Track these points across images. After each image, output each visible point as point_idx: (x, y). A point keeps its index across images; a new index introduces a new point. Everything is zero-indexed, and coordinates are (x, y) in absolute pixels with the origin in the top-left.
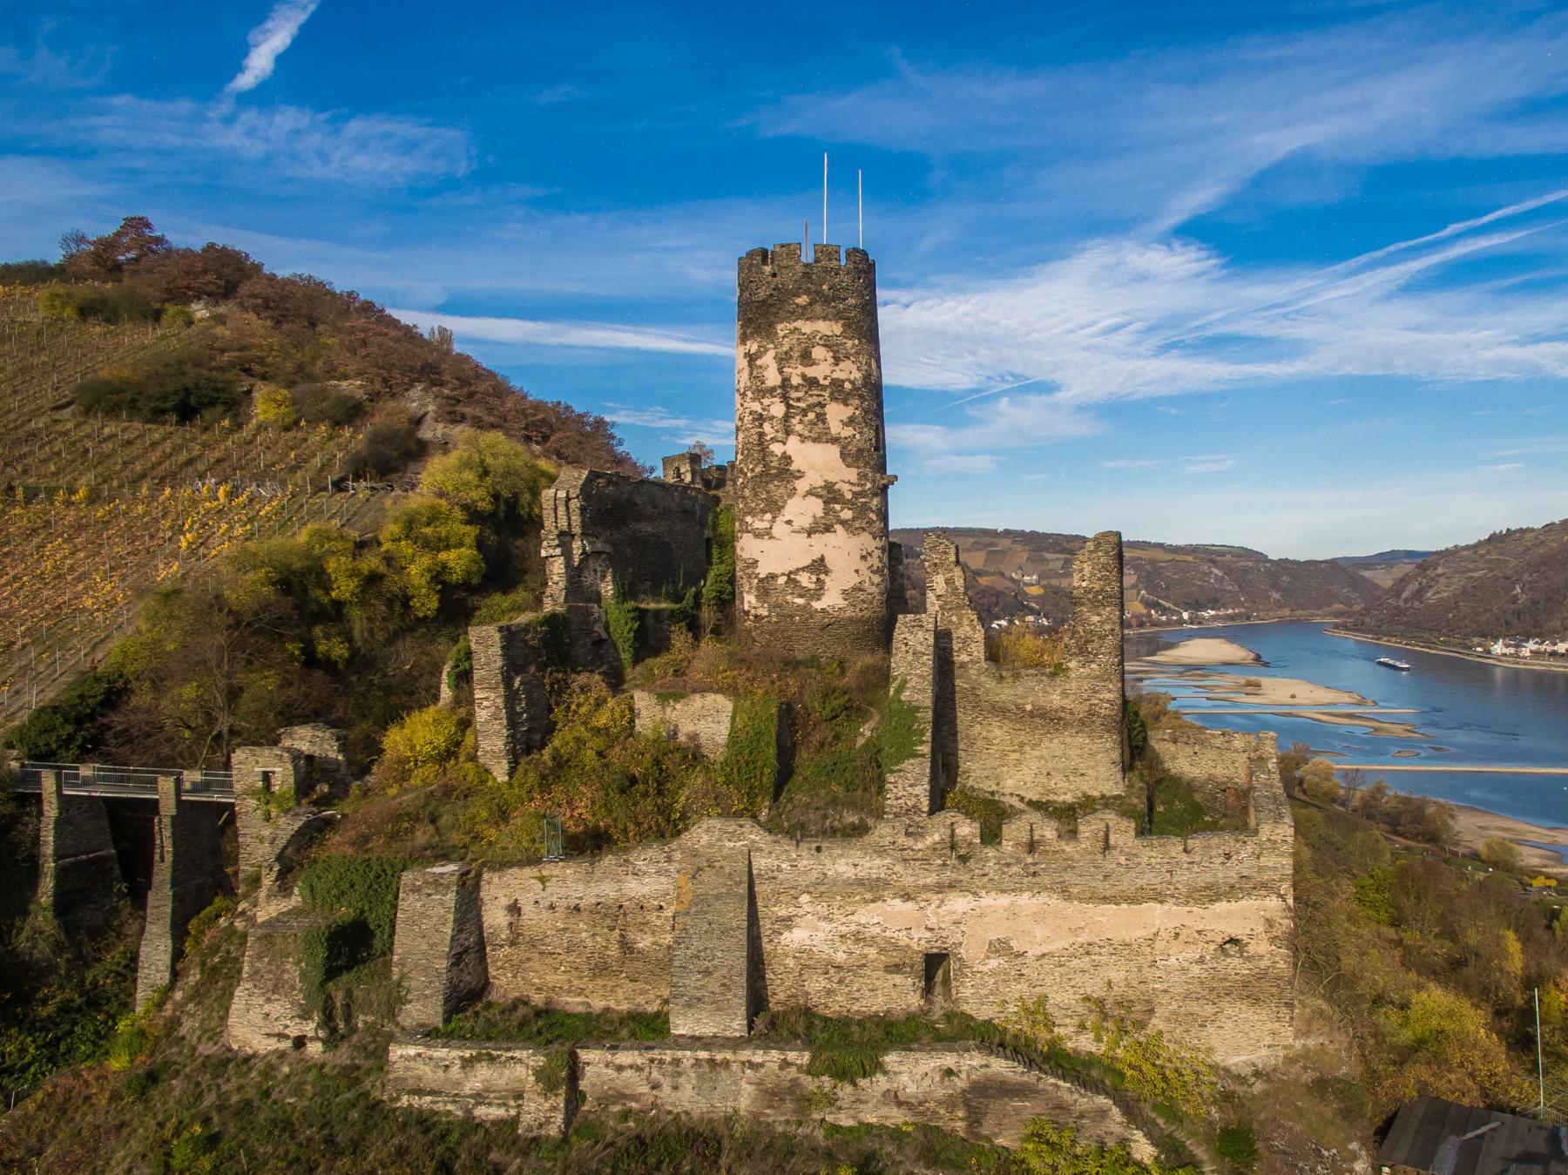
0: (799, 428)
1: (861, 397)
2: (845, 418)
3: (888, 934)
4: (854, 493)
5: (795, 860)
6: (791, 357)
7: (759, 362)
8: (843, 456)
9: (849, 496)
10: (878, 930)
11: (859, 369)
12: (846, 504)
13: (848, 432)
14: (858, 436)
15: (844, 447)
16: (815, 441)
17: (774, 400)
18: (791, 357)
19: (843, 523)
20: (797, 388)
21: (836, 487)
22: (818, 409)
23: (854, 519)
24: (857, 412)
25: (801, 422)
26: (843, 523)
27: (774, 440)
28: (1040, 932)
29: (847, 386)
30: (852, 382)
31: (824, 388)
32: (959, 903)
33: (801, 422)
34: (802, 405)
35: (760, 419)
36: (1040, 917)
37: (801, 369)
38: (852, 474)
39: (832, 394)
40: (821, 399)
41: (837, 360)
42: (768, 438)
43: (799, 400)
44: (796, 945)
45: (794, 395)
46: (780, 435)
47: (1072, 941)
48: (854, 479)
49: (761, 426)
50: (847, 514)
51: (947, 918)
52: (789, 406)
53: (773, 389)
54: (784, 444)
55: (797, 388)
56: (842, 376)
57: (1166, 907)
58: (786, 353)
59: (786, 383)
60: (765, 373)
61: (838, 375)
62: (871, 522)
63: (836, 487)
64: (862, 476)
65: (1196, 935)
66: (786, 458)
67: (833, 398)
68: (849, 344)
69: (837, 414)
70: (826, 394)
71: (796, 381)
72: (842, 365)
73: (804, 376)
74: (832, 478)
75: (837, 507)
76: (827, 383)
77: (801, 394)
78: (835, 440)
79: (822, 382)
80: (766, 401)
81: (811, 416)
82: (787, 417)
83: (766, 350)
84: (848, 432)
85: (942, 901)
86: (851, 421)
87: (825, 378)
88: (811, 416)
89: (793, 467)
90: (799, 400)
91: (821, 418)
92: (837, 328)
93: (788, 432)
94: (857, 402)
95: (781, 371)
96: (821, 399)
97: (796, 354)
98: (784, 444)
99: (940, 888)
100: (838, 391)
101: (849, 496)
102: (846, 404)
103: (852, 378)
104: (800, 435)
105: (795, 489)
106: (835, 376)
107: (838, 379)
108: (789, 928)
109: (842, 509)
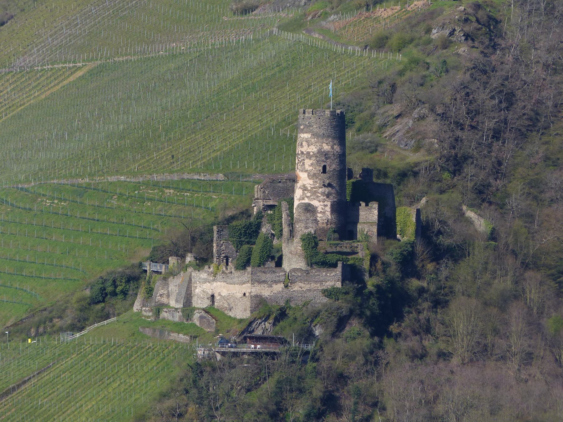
1: (317, 157)
2: (310, 164)
8: (308, 176)
9: (309, 188)
11: (316, 148)
12: (308, 191)
14: (314, 169)
15: (309, 173)
19: (307, 197)
22: (303, 161)
23: (311, 196)
26: (307, 197)
29: (311, 153)
38: (311, 182)
41: (309, 146)
50: (309, 194)
62: (318, 197)
67: (307, 158)
68: (313, 140)
72: (310, 147)
75: (306, 192)
78: (306, 171)
81: (302, 163)
84: (311, 168)
86: (312, 164)
88: (302, 163)
91: (304, 163)
94: (314, 158)
101: (309, 188)
102: (310, 159)
103: (313, 151)
106: (308, 151)
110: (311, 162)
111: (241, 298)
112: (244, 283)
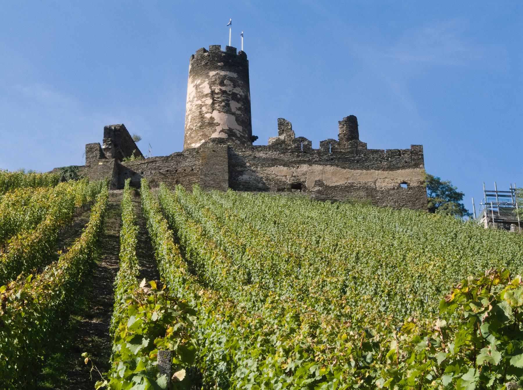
0: (218, 108)
3: (278, 177)
4: (241, 135)
5: (245, 152)
6: (216, 83)
7: (201, 86)
8: (237, 120)
10: (274, 176)
13: (239, 112)
14: (243, 116)
16: (224, 112)
17: (207, 98)
18: (216, 83)
20: (217, 94)
21: (234, 131)
24: (242, 107)
25: (219, 106)
27: (206, 113)
28: (334, 179)
30: (241, 96)
31: (229, 95)
32: (305, 168)
33: (219, 106)
34: (220, 100)
35: (201, 106)
36: (334, 174)
37: (219, 87)
38: (240, 128)
39: (232, 97)
40: (228, 98)
41: (235, 86)
42: (204, 112)
43: (218, 98)
44: (244, 181)
45: (216, 96)
46: (210, 111)
47: (346, 182)
48: (241, 130)
49: (201, 109)
51: (300, 173)
52: (214, 100)
53: (206, 95)
54: (211, 113)
55: (217, 94)
56: (237, 92)
57: (379, 171)
58: (214, 81)
59: (213, 93)
60: (204, 90)
61: (235, 91)
63: (234, 131)
64: (244, 130)
65: (391, 181)
66: (212, 118)
67: (233, 99)
68: (240, 82)
69: (234, 105)
70: (230, 97)
71: (217, 91)
72: (236, 88)
73: (220, 90)
74: (232, 127)
75: (234, 138)
76: (230, 93)
77: (219, 96)
78: (233, 114)
79: (228, 92)
80: (203, 100)
82: (213, 104)
83: (205, 81)
84: (239, 112)
85: (298, 167)
86: (239, 109)
87: (230, 91)
89: (215, 122)
90: (218, 98)
92: (235, 75)
93: (213, 110)
95: (210, 87)
96: (228, 98)
97: (218, 82)
98: (211, 113)
99: (295, 162)
100: (234, 96)
101: (239, 136)
103: (241, 94)
104: (218, 110)
105: (216, 130)
107: (235, 93)
108: (242, 175)
109: (236, 140)
110: (239, 105)
111: (394, 189)
112: (398, 168)
